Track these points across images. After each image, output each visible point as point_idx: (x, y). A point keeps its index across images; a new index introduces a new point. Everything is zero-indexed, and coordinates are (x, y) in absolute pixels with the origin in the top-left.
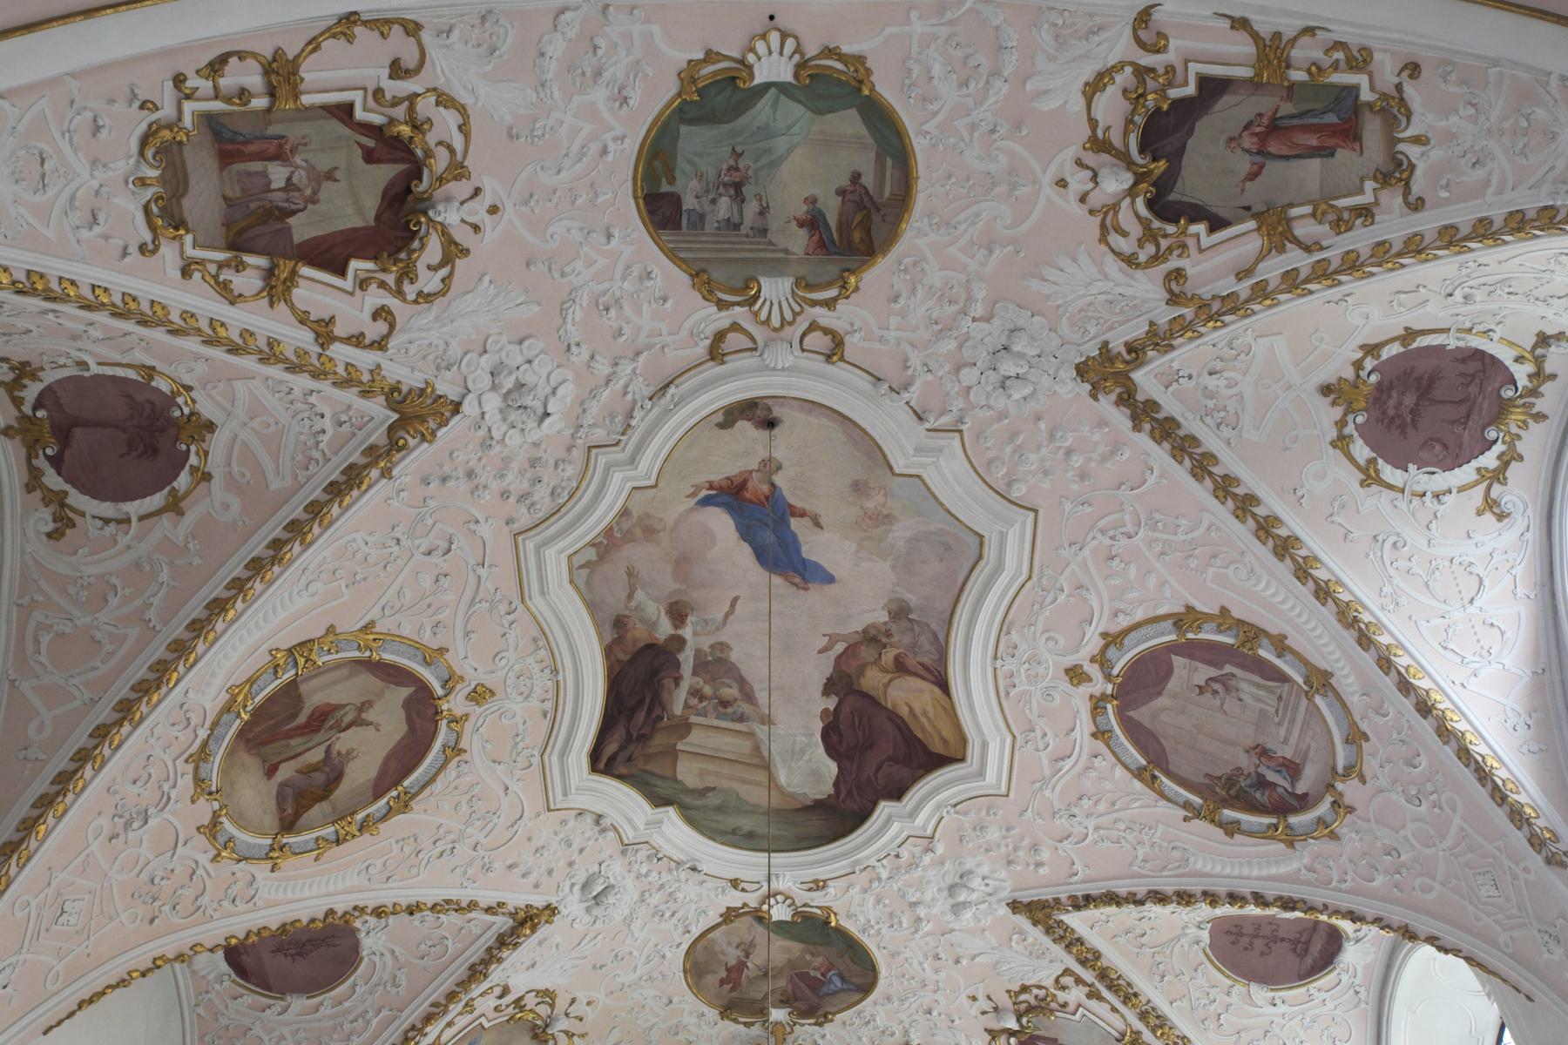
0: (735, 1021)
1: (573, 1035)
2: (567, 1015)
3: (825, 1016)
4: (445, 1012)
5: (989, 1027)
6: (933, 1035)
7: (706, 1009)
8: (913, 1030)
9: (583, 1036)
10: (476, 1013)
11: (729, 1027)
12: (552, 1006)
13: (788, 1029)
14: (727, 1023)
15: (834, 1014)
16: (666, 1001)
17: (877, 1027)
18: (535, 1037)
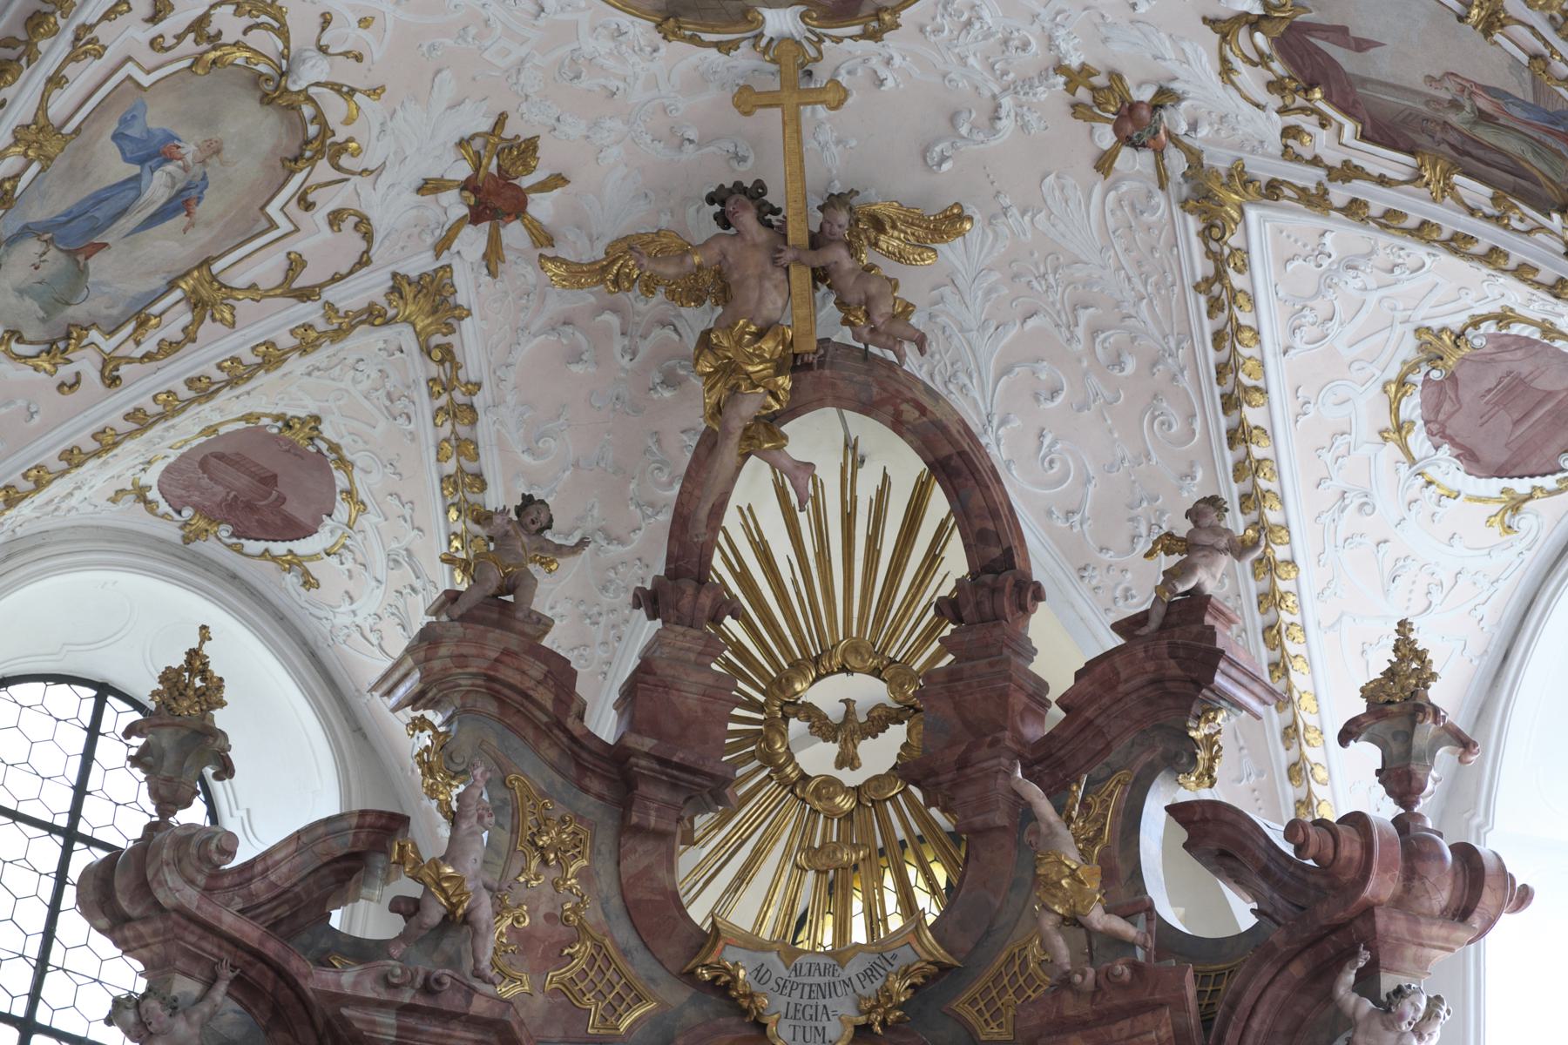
0: (694, 40)
1: (352, 91)
2: (323, 50)
3: (877, 15)
4: (32, 56)
5: (1211, 15)
6: (1106, 40)
7: (624, 20)
8: (1061, 32)
9: (375, 92)
10: (110, 57)
11: (684, 58)
12: (283, 32)
13: (812, 52)
14: (678, 46)
15: (895, 11)
16: (533, 9)
17: (988, 35)
18: (266, 100)
